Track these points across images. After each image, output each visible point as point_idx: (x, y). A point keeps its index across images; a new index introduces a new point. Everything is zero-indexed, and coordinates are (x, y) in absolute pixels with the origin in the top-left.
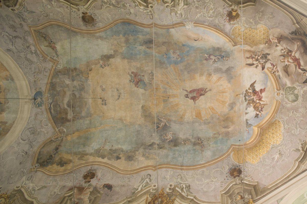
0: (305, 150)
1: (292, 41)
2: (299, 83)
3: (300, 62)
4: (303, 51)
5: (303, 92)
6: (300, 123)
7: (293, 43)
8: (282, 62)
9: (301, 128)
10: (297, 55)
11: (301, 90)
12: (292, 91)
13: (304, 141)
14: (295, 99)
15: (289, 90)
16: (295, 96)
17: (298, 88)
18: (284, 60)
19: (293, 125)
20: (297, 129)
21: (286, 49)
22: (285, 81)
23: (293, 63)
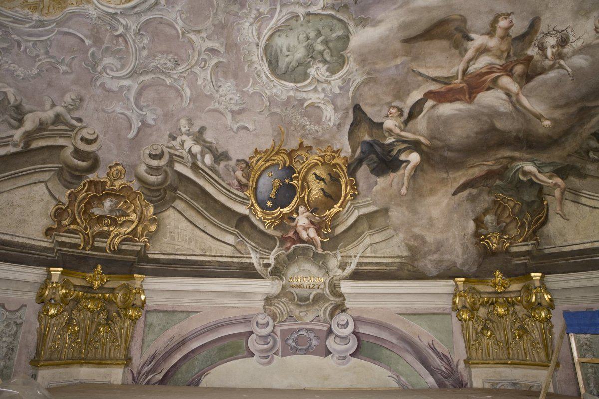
0: (35, 145)
1: (579, 105)
2: (358, 88)
3: (458, 100)
4: (499, 125)
5: (313, 105)
6: (166, 86)
7: (563, 102)
8: (495, 21)
9: (139, 94)
10: (490, 99)
11: (322, 96)
12: (322, 53)
13: (80, 120)
14: (282, 65)
15: (334, 35)
16: (299, 64)
17: (336, 81)
18: (499, 32)
19: (145, 53)
20: (131, 76)
21: (551, 63)
22: (380, 22)
23: (465, 72)
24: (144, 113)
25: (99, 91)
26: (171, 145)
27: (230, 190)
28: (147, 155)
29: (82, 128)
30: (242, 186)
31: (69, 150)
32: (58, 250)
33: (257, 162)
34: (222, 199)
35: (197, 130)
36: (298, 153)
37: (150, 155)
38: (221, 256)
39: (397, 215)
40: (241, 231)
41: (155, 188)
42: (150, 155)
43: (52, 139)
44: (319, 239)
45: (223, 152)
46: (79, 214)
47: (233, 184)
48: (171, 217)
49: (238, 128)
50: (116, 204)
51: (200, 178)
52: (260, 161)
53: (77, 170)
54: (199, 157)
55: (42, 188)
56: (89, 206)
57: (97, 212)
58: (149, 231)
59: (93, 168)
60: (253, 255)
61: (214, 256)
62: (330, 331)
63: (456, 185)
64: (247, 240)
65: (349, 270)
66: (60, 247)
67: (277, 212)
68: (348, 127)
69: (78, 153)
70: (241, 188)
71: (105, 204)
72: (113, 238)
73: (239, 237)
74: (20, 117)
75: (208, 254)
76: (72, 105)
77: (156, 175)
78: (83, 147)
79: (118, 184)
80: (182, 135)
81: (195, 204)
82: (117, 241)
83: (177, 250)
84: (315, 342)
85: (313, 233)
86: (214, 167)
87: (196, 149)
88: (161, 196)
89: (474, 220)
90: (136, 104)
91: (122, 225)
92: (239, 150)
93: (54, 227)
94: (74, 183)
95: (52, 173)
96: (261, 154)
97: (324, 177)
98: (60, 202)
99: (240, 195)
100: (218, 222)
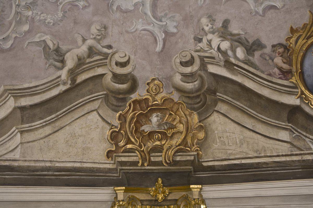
0: (80, 79)
13: (110, 47)
24: (164, 23)
25: (118, 15)
26: (199, 48)
27: (274, 81)
28: (179, 64)
29: (114, 54)
30: (286, 74)
31: (109, 77)
32: (121, 170)
33: (296, 42)
34: (266, 92)
35: (221, 25)
37: (181, 63)
38: (278, 156)
40: (295, 125)
41: (195, 95)
42: (181, 63)
43: (92, 71)
45: (254, 41)
46: (132, 133)
47: (275, 73)
49: (265, 10)
50: (162, 118)
51: (237, 75)
52: (300, 41)
53: (120, 94)
54: (230, 53)
55: (94, 116)
56: (138, 125)
57: (146, 128)
58: (198, 139)
59: (133, 88)
61: (270, 156)
64: (304, 134)
66: (121, 166)
69: (117, 78)
70: (285, 76)
71: (152, 120)
72: (167, 151)
73: (294, 132)
74: (61, 58)
75: (263, 155)
76: (99, 35)
77: (192, 82)
79: (159, 97)
80: (206, 34)
81: (238, 103)
82: (171, 153)
83: (231, 154)
86: (249, 60)
87: (225, 45)
88: (202, 102)
90: (154, 17)
91: (172, 137)
93: (113, 149)
94: (120, 106)
95: (100, 101)
96: (299, 32)
98: (113, 126)
99: (286, 84)
100: (266, 118)
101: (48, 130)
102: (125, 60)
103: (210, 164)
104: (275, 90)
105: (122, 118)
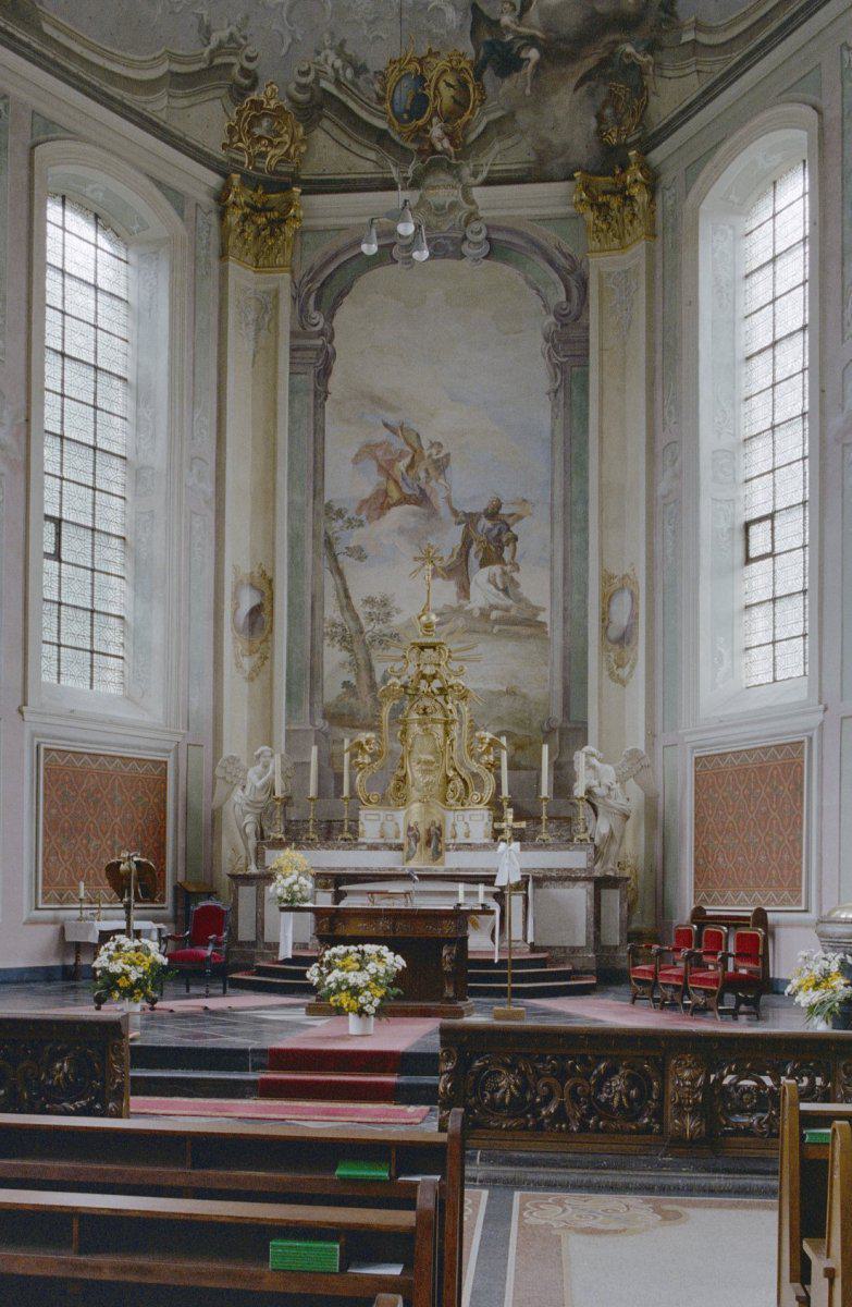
0: (218, 61)
29: (247, 45)
31: (236, 69)
33: (393, 71)
34: (364, 115)
36: (428, 59)
39: (524, 118)
44: (452, 149)
48: (320, 138)
50: (272, 124)
53: (242, 88)
54: (341, 72)
57: (258, 131)
59: (253, 87)
60: (393, 169)
62: (465, 238)
63: (574, 81)
65: (480, 178)
67: (414, 123)
68: (469, 27)
69: (245, 72)
78: (247, 65)
79: (273, 102)
80: (325, 49)
82: (273, 162)
84: (451, 249)
85: (446, 144)
89: (596, 117)
91: (276, 147)
92: (376, 59)
97: (452, 82)
101: (185, 102)
102: (254, 55)
103: (307, 177)
104: (371, 114)
105: (239, 113)
